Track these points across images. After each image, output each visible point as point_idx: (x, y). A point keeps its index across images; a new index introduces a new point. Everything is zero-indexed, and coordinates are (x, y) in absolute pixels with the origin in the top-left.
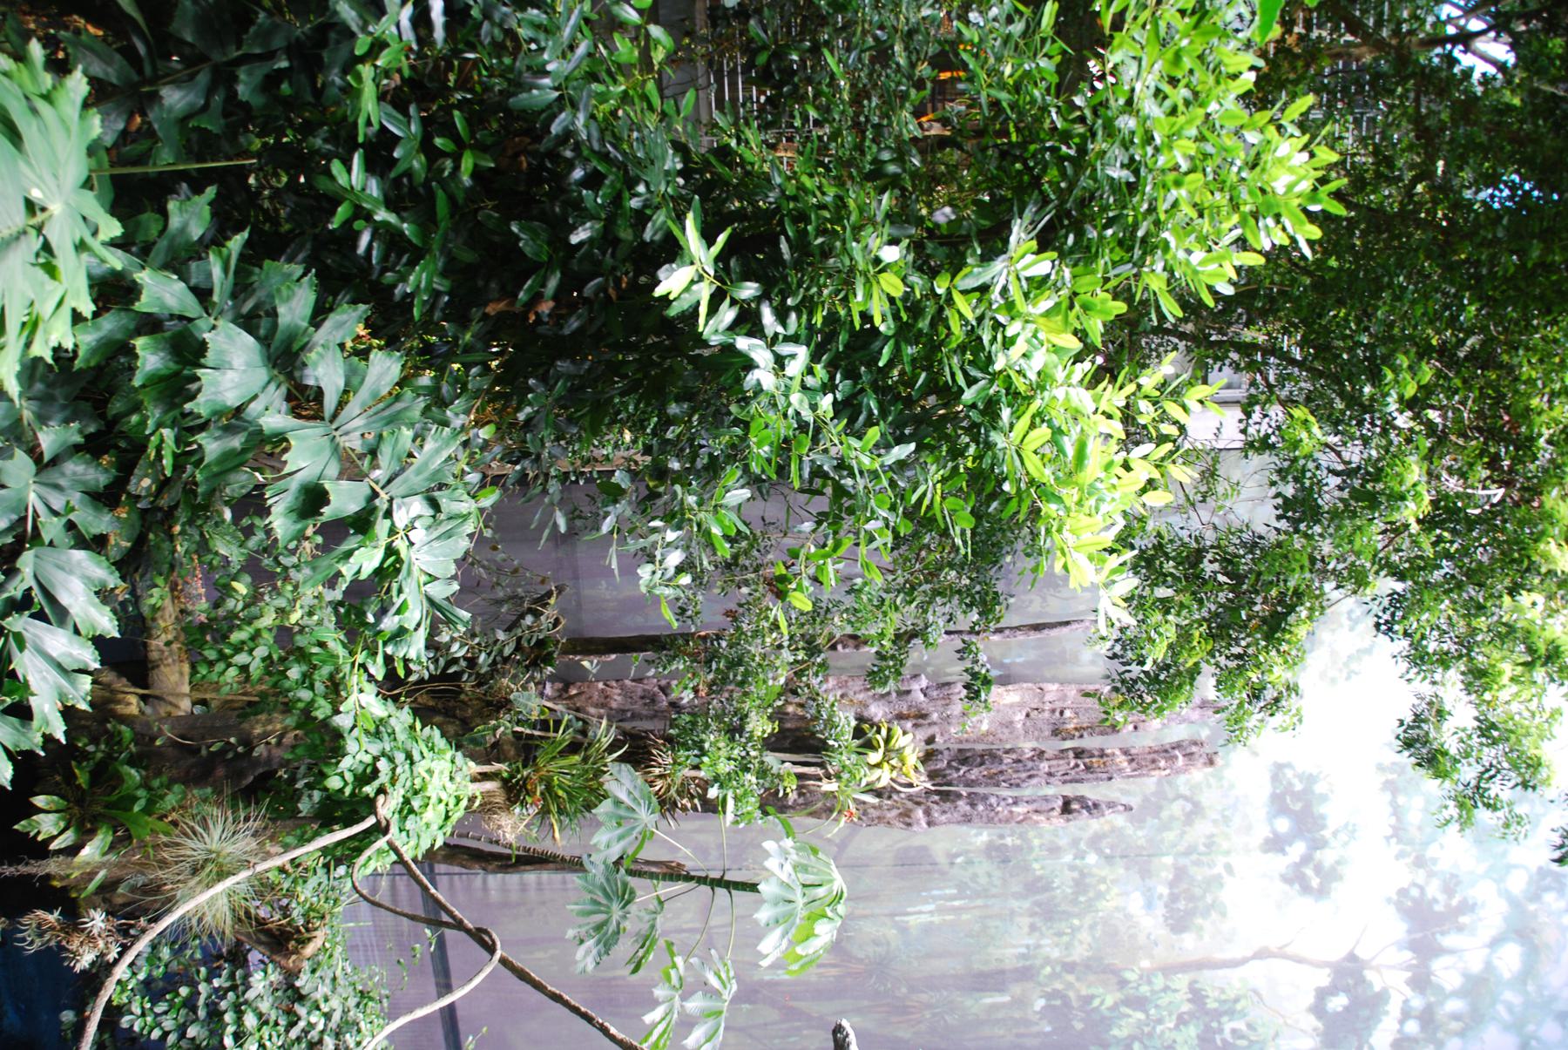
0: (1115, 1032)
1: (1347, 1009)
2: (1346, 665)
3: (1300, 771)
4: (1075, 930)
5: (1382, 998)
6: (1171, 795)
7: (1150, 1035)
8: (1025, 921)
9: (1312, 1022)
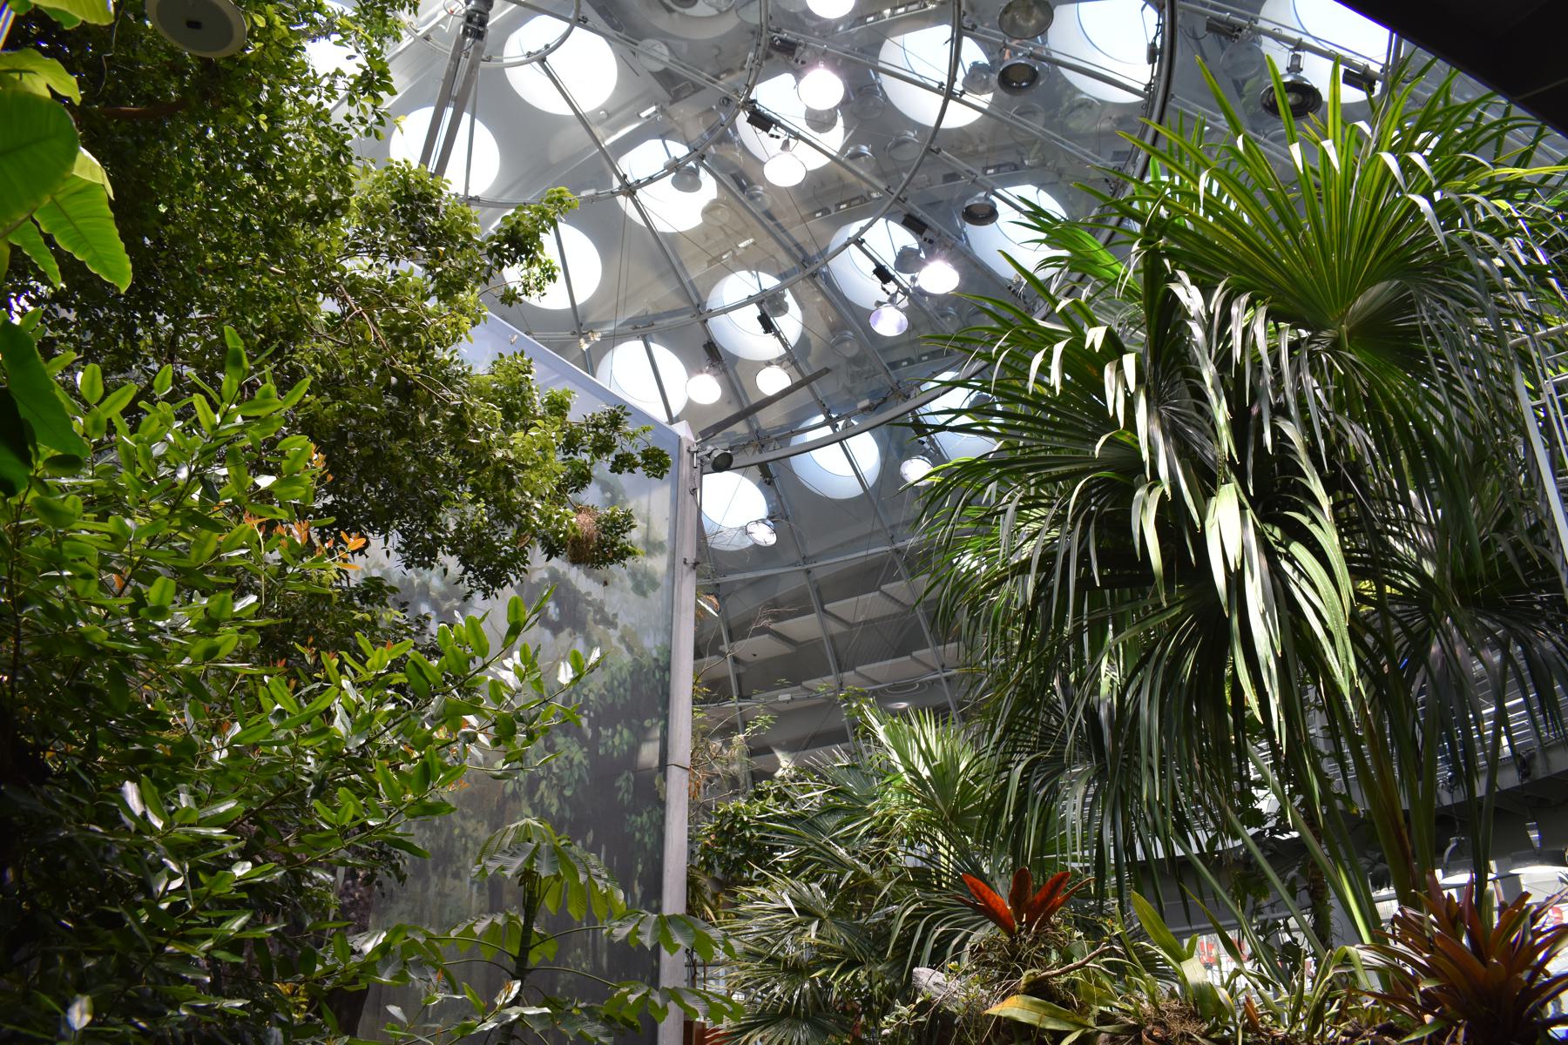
0: (554, 810)
1: (558, 605)
4: (463, 834)
5: (554, 576)
7: (560, 779)
8: (450, 882)
9: (564, 635)
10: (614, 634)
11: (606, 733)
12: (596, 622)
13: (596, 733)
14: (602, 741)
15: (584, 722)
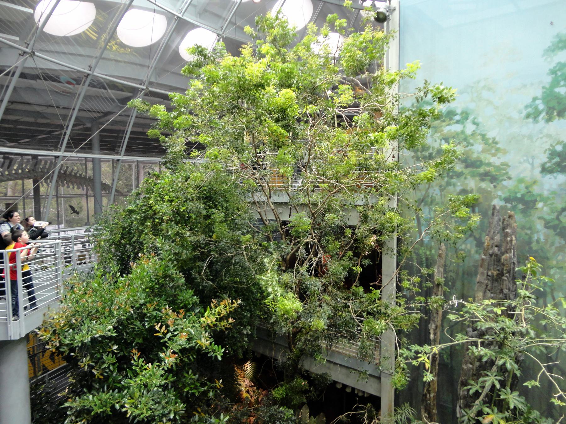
2: (489, 145)
3: (547, 160)
6: (557, 222)
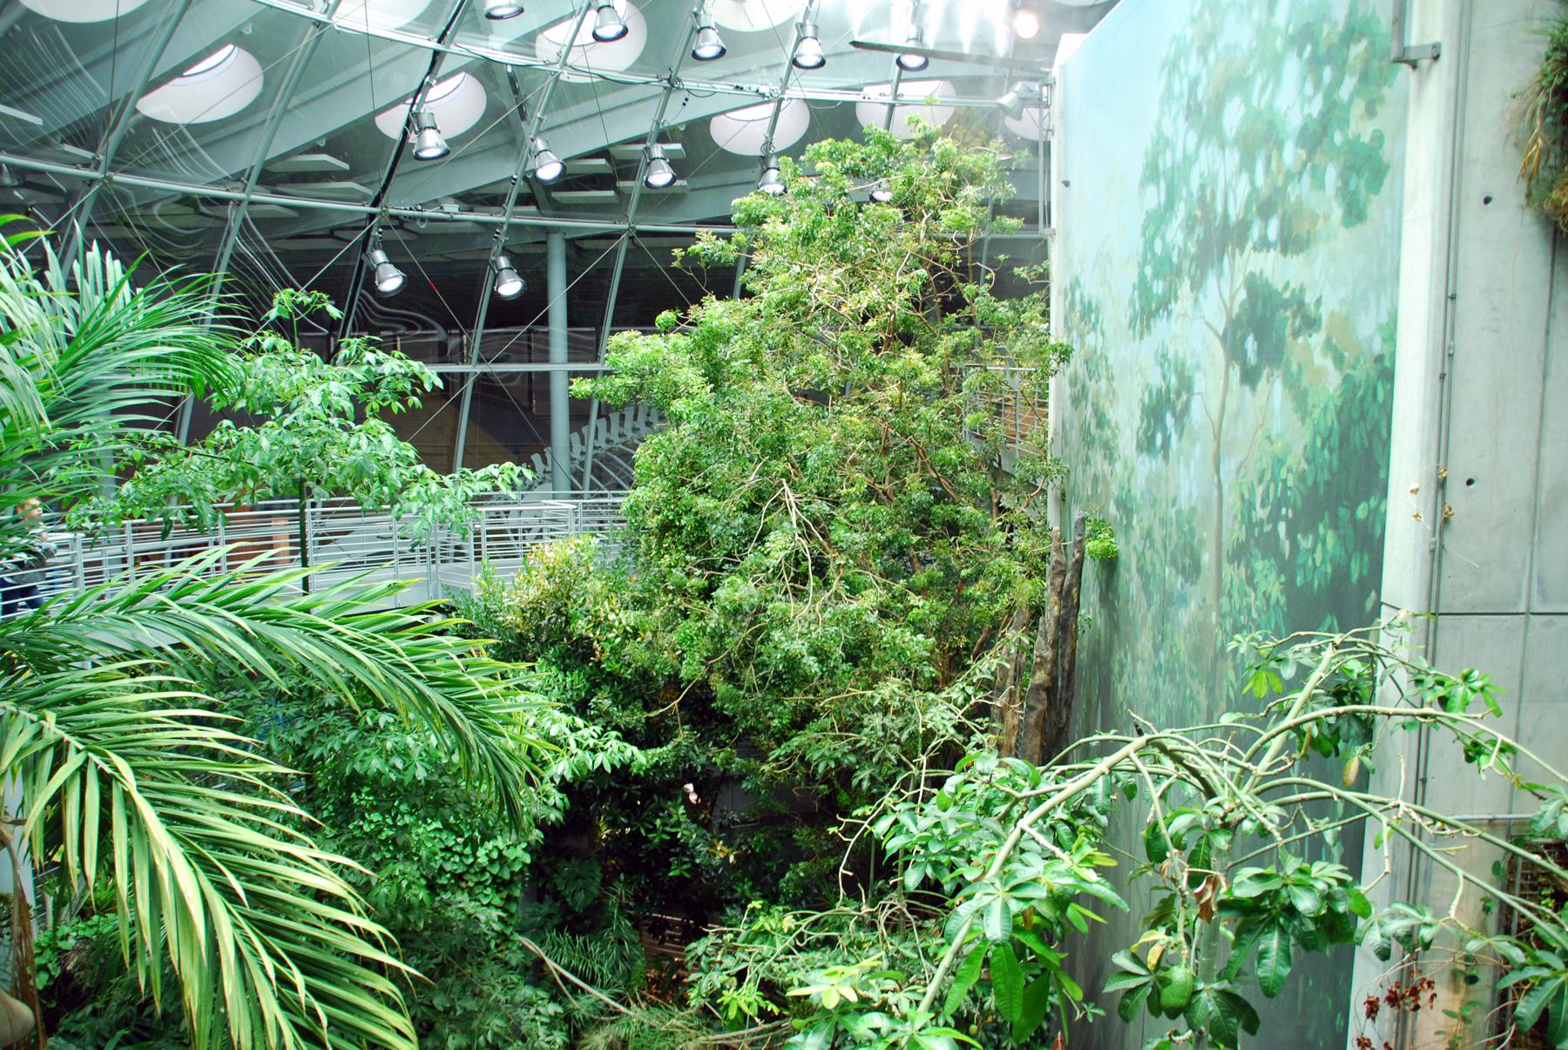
10: (1317, 339)
11: (1305, 543)
12: (1295, 335)
13: (1295, 546)
14: (1300, 561)
15: (1282, 528)
